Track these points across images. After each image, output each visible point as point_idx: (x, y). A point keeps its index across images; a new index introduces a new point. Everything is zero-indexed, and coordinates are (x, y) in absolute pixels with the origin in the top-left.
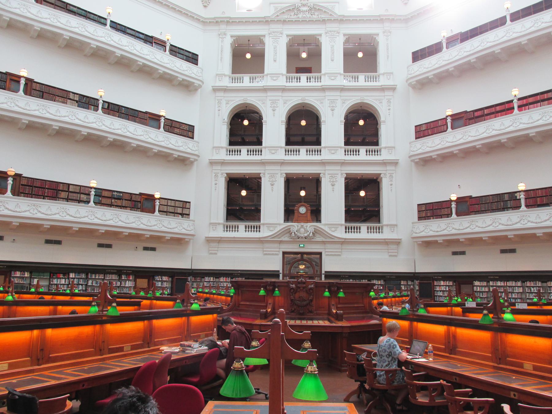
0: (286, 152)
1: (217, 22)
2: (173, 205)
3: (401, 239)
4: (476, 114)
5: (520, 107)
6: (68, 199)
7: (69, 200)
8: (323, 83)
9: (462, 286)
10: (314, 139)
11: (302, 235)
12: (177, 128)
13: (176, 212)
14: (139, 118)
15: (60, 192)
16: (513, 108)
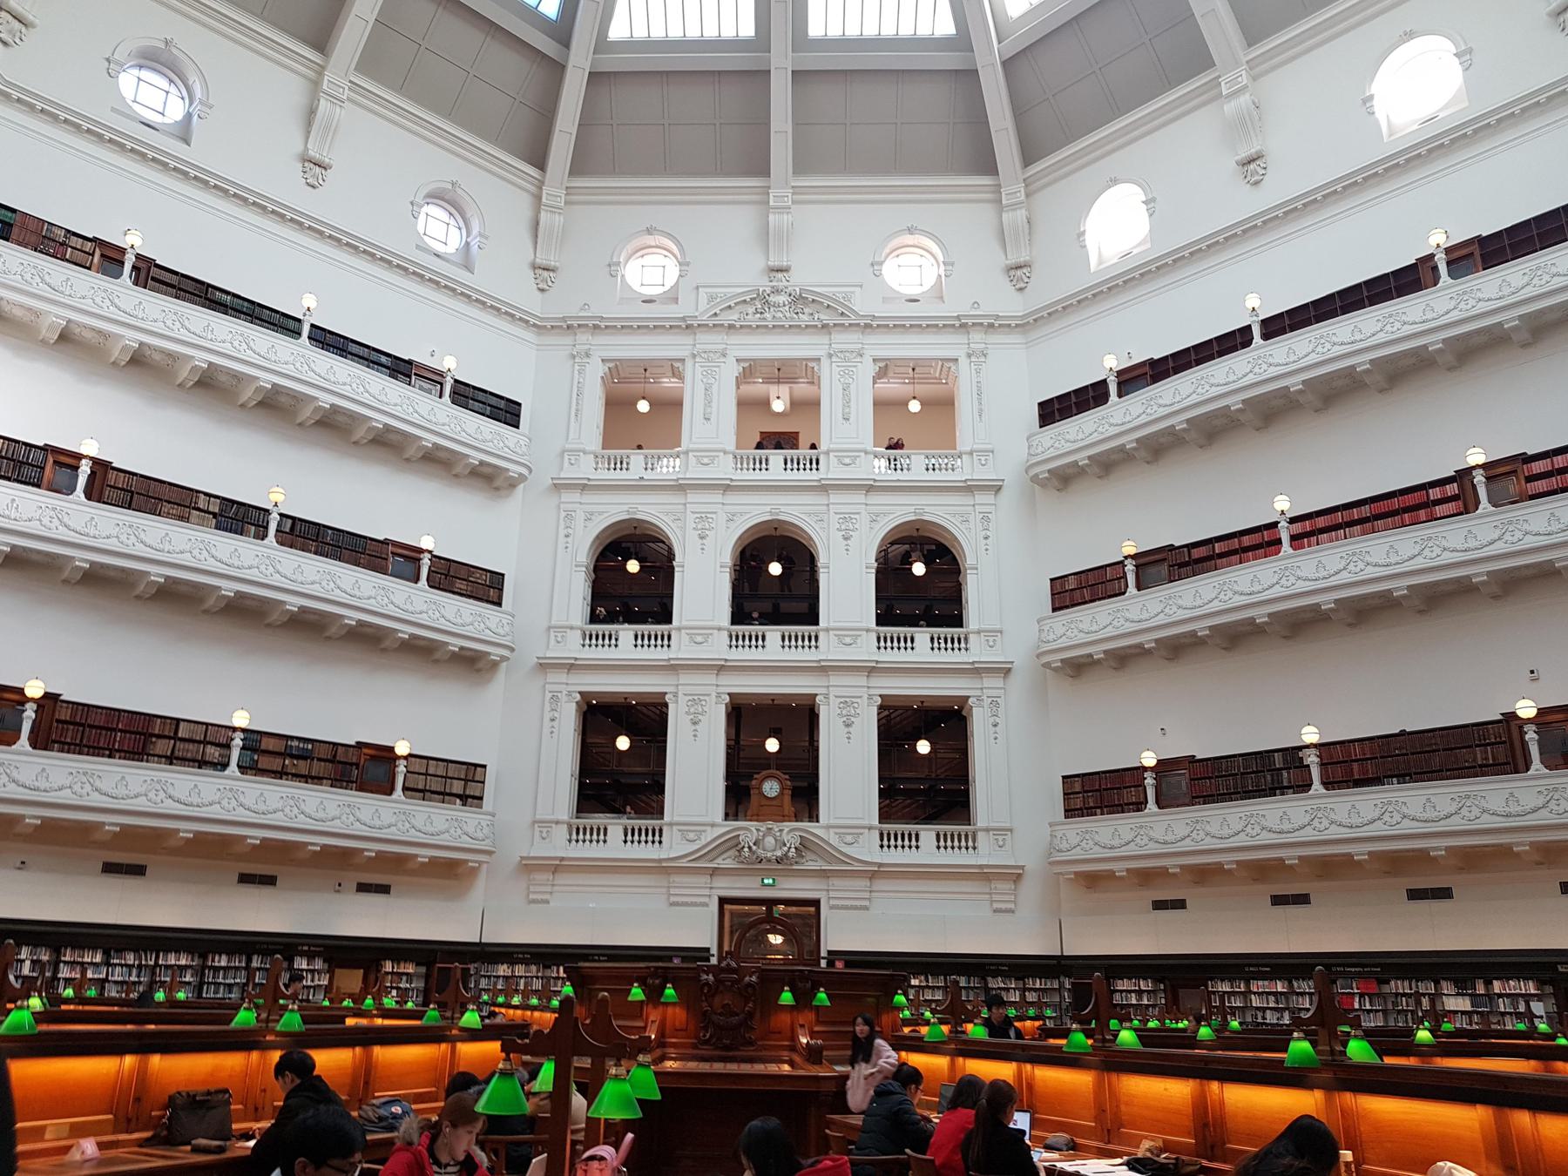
1: (569, 327)
3: (1022, 867)
4: (1196, 553)
5: (1295, 539)
6: (171, 759)
7: (175, 761)
8: (822, 474)
10: (803, 607)
11: (769, 855)
12: (460, 579)
13: (448, 791)
14: (368, 555)
15: (154, 739)
16: (1279, 542)
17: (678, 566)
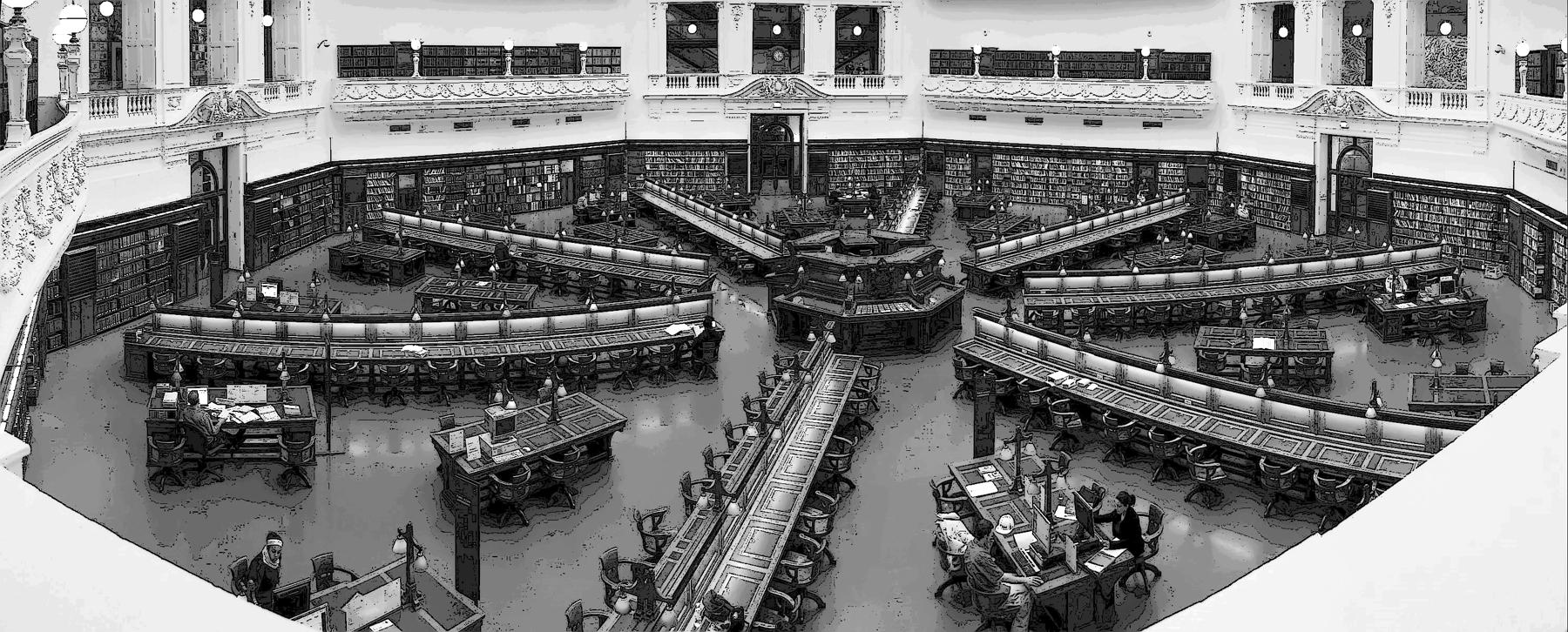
2: (599, 54)
9: (980, 158)
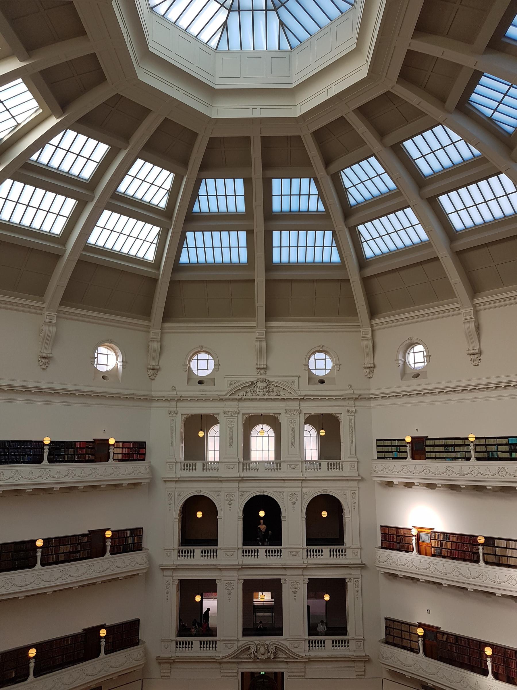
0: (243, 553)
17: (219, 519)
